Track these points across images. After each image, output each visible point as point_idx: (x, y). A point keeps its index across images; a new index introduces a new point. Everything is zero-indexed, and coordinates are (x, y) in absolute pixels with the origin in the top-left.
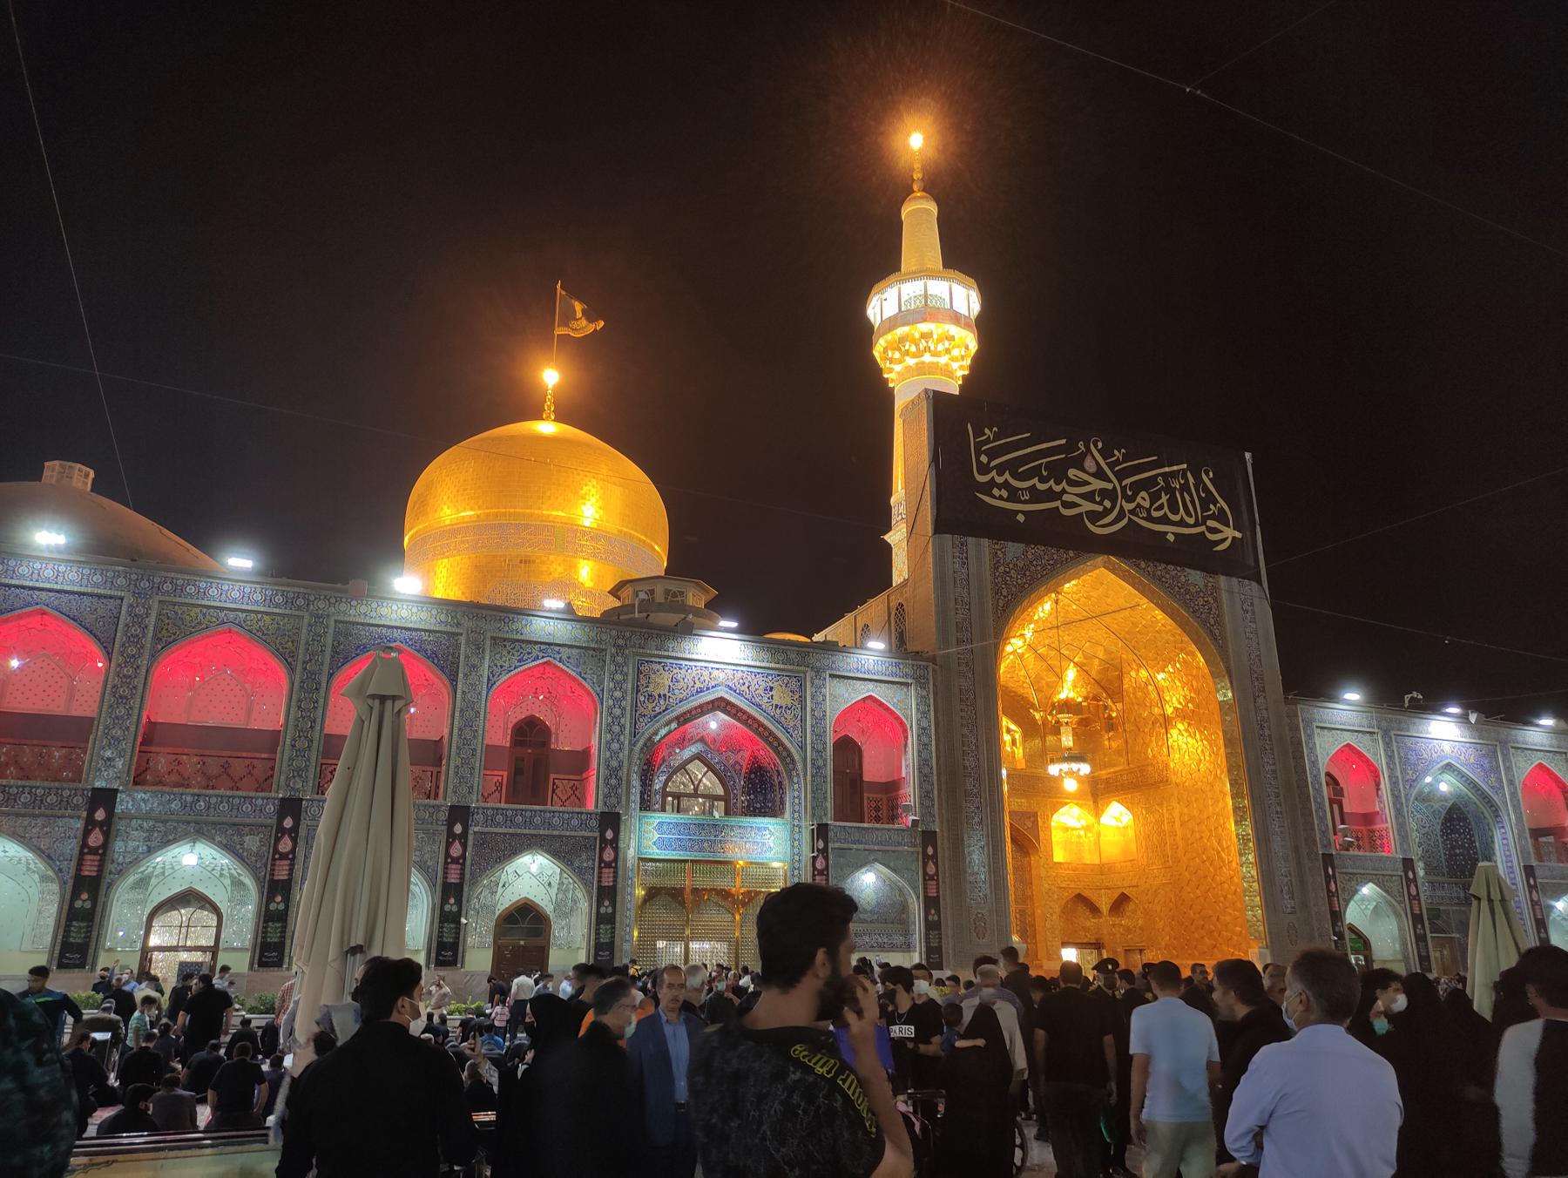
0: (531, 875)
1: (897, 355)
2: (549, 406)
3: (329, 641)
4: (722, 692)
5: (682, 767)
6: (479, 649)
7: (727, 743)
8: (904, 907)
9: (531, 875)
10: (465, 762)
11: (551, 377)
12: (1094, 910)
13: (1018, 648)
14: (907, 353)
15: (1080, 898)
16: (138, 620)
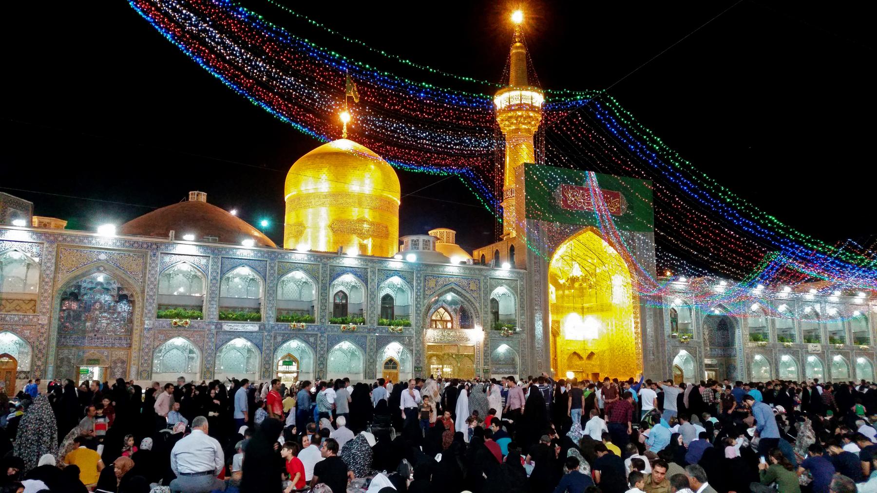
0: (393, 350)
1: (507, 123)
2: (345, 130)
3: (328, 272)
4: (453, 286)
5: (436, 310)
6: (374, 273)
7: (453, 302)
8: (513, 360)
9: (393, 350)
10: (372, 313)
11: (345, 117)
12: (580, 358)
13: (556, 263)
14: (512, 123)
15: (575, 353)
16: (272, 268)
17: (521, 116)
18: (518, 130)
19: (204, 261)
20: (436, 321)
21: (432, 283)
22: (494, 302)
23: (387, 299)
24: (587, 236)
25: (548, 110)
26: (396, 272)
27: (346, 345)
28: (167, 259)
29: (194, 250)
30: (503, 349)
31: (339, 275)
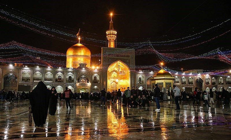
2: (79, 42)
11: (79, 39)
17: (110, 36)
18: (110, 39)
19: (30, 71)
20: (82, 81)
21: (79, 74)
22: (95, 77)
23: (70, 77)
24: (120, 63)
25: (117, 35)
26: (70, 72)
27: (59, 86)
28: (23, 70)
29: (28, 69)
30: (96, 87)
31: (58, 73)
